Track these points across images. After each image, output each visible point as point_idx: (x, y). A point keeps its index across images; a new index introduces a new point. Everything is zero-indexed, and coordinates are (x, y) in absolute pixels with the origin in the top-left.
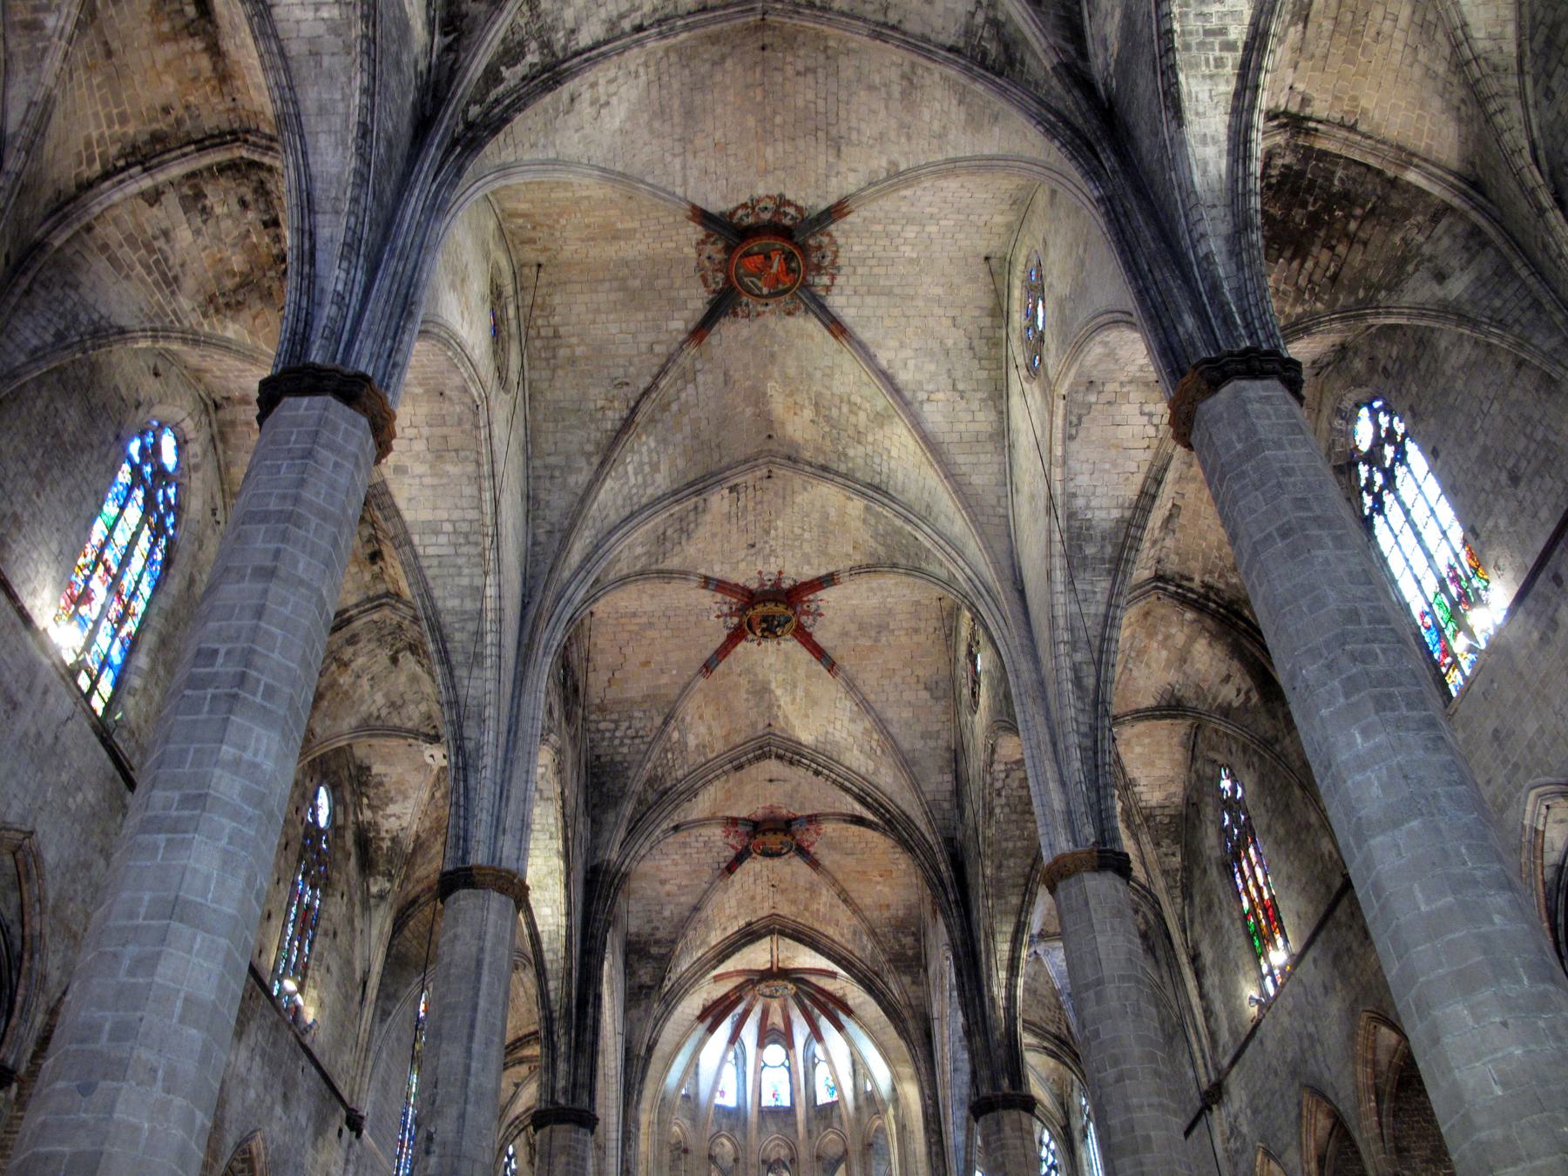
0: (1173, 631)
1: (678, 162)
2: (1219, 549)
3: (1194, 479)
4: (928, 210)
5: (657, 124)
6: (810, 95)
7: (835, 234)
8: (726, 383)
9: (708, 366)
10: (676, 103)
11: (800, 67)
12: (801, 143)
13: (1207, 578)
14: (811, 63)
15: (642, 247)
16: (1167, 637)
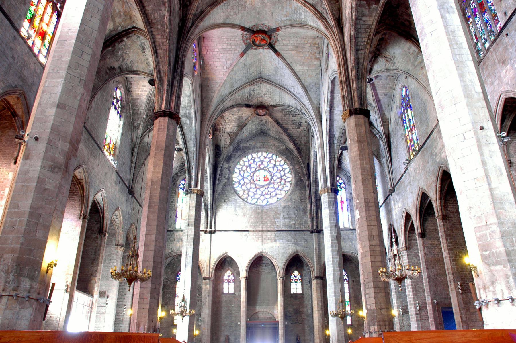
0: (120, 20)
1: (280, 65)
2: (128, 55)
3: (144, 61)
4: (222, 55)
5: (283, 75)
6: (251, 70)
7: (243, 44)
8: (272, 13)
9: (277, 20)
10: (279, 75)
11: (253, 74)
12: (252, 61)
13: (124, 43)
14: (251, 76)
15: (291, 42)
16: (120, 16)
